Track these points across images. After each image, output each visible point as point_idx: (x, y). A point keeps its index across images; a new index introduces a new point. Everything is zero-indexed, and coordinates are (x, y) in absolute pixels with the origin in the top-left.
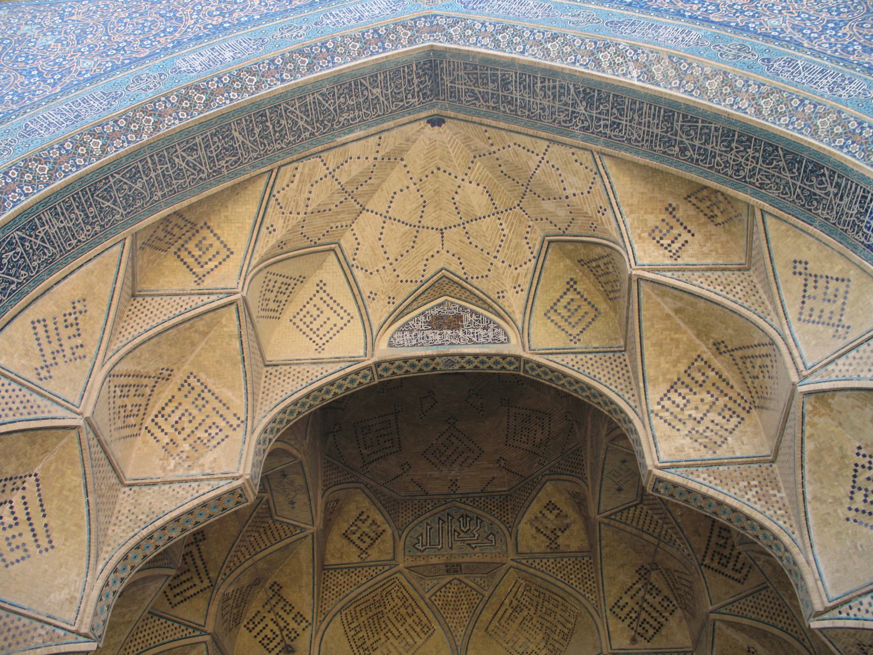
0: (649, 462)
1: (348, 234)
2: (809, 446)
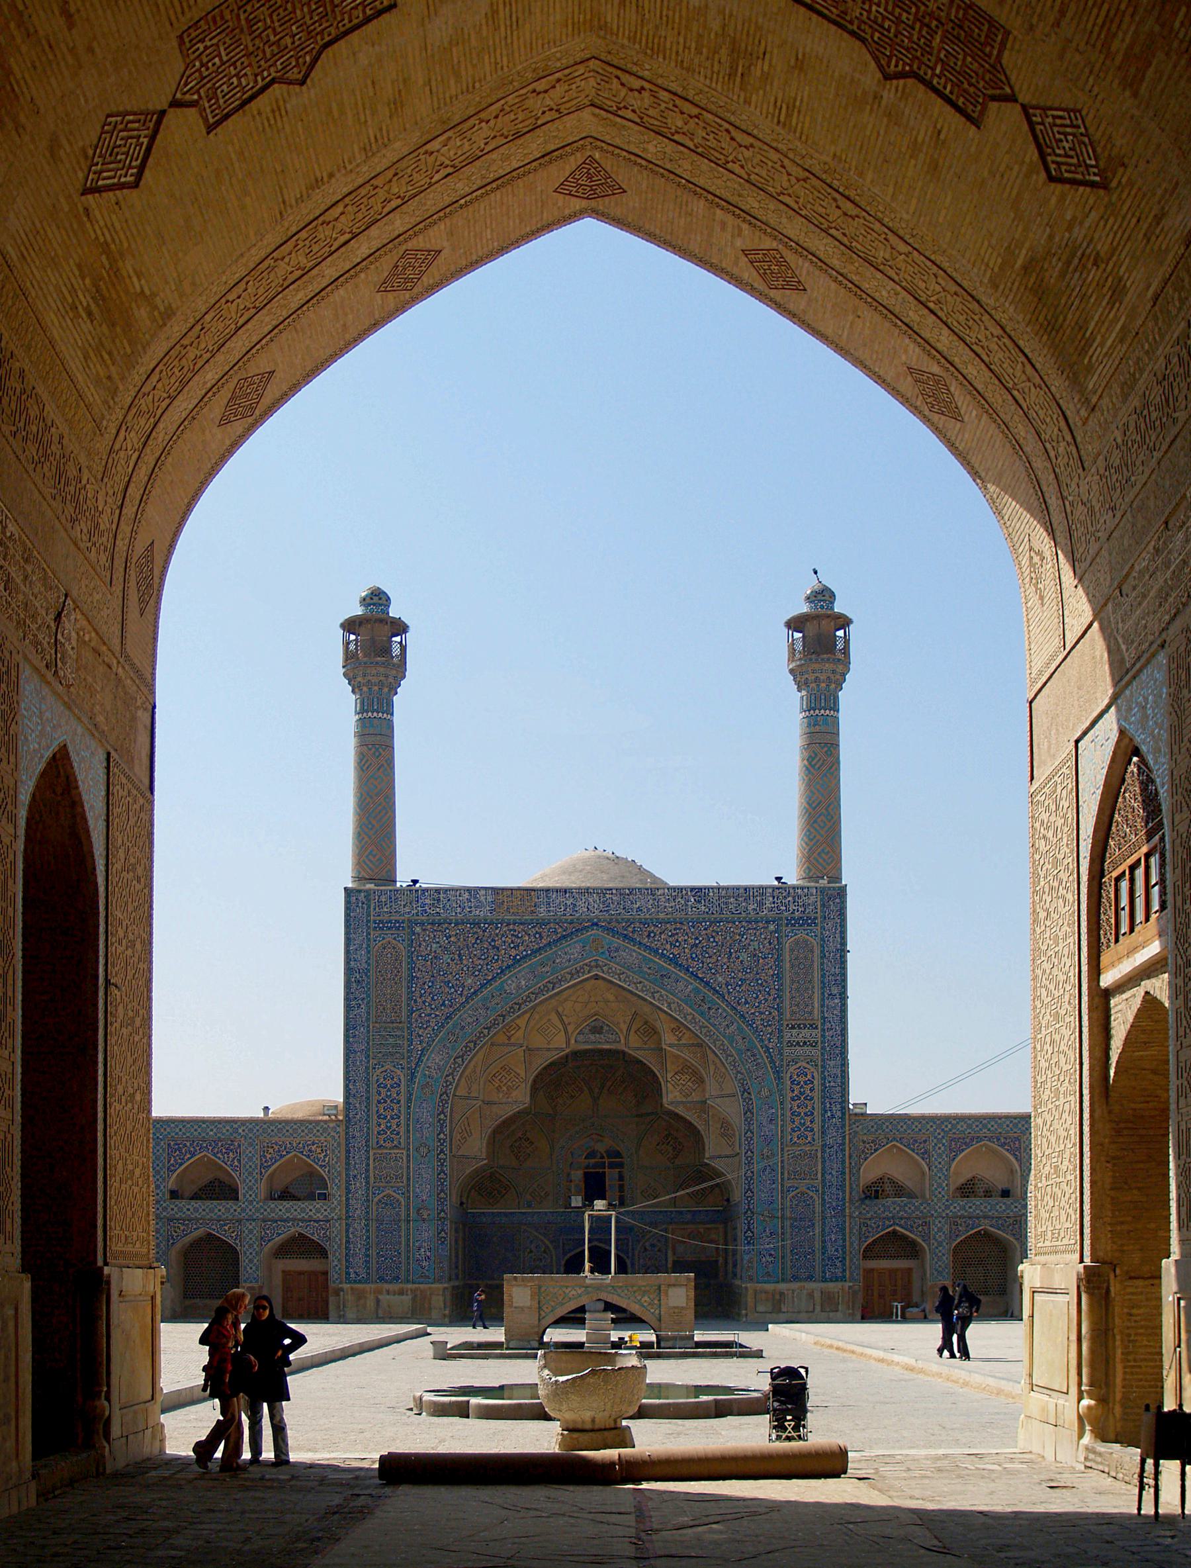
0: (664, 1100)
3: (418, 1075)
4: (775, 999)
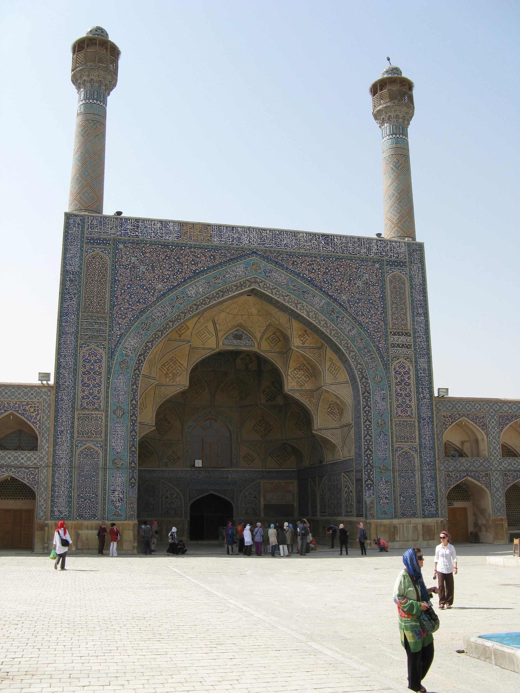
1: (217, 317)
2: (322, 397)
3: (117, 354)
4: (381, 314)
